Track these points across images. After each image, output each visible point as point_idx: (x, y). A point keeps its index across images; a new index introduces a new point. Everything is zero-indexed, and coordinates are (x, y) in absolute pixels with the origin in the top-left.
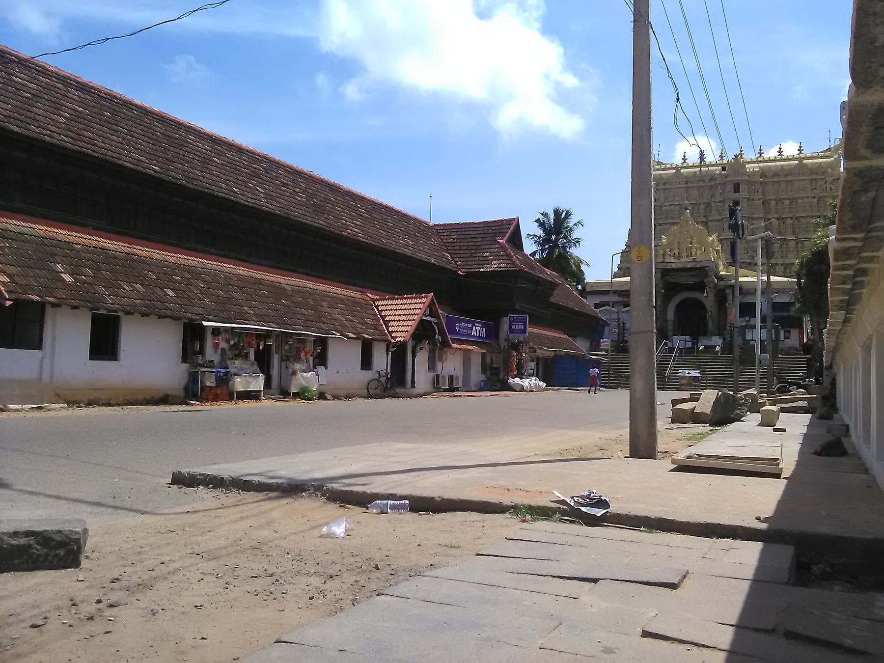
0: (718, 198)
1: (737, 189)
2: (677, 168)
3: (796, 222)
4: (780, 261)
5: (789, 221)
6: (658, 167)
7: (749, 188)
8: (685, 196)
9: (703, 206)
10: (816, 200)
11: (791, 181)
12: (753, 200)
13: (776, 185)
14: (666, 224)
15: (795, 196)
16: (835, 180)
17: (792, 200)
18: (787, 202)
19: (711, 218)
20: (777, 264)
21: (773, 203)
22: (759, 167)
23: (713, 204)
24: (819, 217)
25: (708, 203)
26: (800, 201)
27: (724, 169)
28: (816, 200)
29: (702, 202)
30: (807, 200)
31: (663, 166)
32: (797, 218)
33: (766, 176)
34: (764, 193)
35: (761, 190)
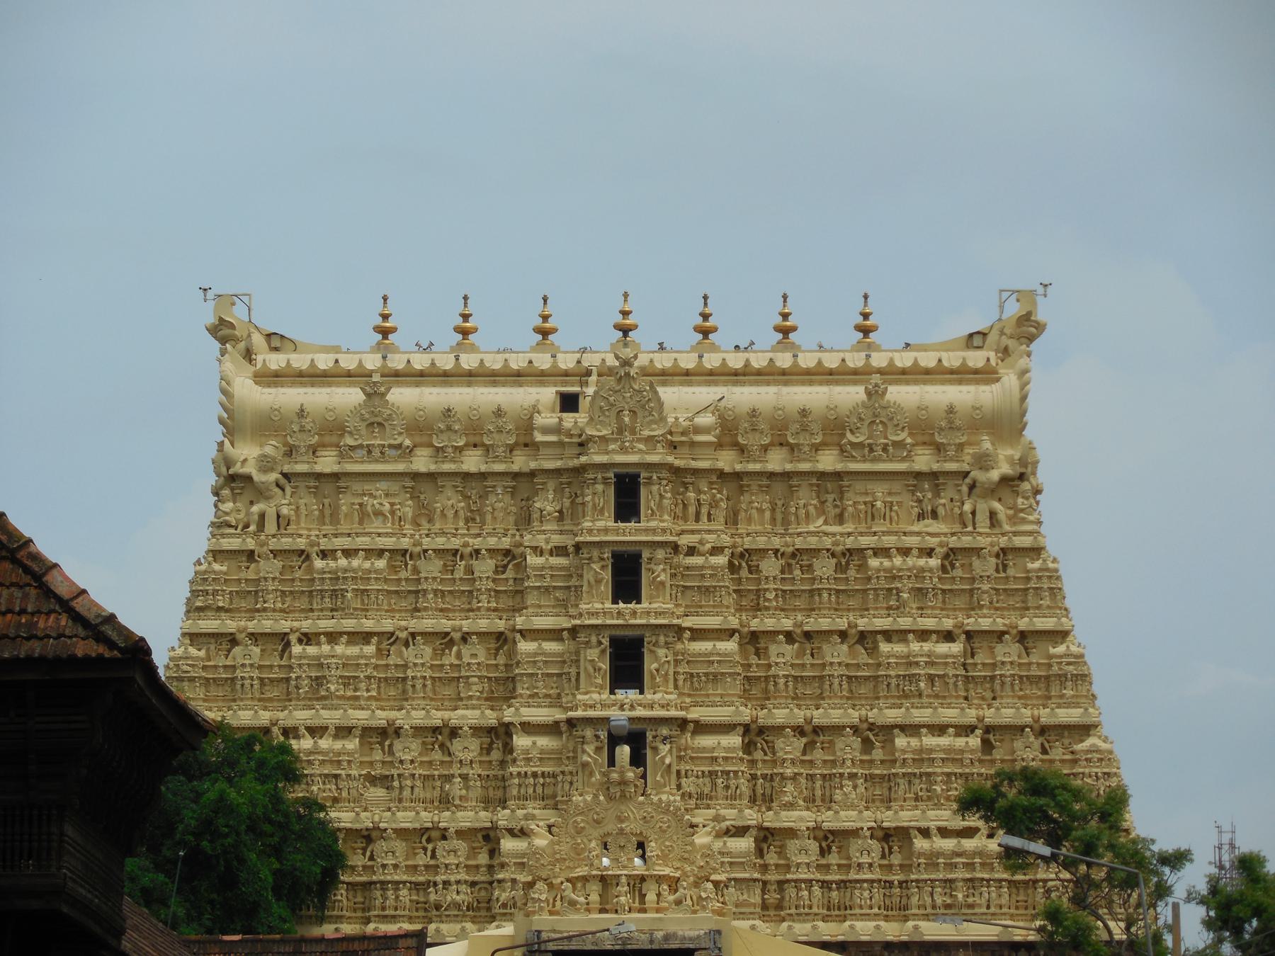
0: (547, 535)
1: (627, 507)
2: (374, 385)
3: (863, 657)
4: (800, 818)
5: (837, 653)
6: (276, 361)
7: (675, 493)
8: (408, 510)
9: (485, 567)
10: (934, 562)
11: (838, 475)
12: (691, 551)
13: (779, 488)
14: (333, 637)
15: (850, 542)
16: (1005, 480)
17: (849, 557)
18: (824, 568)
19: (520, 622)
20: (791, 833)
21: (770, 567)
22: (713, 407)
23: (533, 560)
24: (948, 636)
25: (507, 553)
26: (874, 563)
27: (569, 403)
28: (934, 562)
29: (476, 543)
30: (898, 561)
31: (300, 361)
32: (863, 637)
33: (742, 450)
34: (733, 519)
35: (720, 515)
